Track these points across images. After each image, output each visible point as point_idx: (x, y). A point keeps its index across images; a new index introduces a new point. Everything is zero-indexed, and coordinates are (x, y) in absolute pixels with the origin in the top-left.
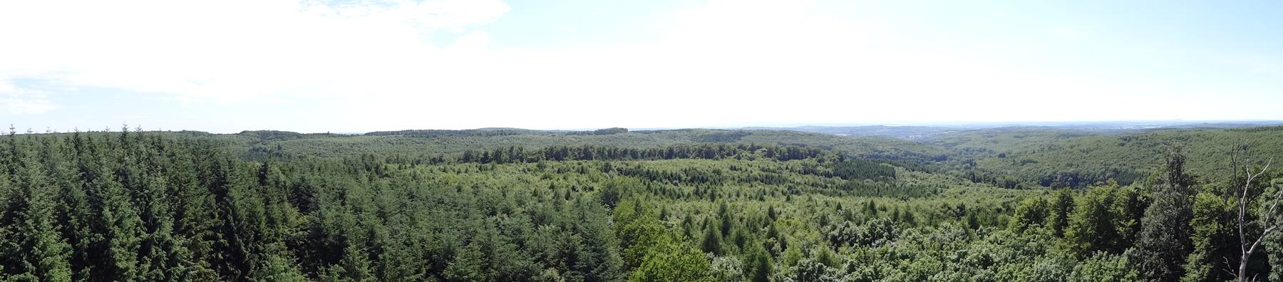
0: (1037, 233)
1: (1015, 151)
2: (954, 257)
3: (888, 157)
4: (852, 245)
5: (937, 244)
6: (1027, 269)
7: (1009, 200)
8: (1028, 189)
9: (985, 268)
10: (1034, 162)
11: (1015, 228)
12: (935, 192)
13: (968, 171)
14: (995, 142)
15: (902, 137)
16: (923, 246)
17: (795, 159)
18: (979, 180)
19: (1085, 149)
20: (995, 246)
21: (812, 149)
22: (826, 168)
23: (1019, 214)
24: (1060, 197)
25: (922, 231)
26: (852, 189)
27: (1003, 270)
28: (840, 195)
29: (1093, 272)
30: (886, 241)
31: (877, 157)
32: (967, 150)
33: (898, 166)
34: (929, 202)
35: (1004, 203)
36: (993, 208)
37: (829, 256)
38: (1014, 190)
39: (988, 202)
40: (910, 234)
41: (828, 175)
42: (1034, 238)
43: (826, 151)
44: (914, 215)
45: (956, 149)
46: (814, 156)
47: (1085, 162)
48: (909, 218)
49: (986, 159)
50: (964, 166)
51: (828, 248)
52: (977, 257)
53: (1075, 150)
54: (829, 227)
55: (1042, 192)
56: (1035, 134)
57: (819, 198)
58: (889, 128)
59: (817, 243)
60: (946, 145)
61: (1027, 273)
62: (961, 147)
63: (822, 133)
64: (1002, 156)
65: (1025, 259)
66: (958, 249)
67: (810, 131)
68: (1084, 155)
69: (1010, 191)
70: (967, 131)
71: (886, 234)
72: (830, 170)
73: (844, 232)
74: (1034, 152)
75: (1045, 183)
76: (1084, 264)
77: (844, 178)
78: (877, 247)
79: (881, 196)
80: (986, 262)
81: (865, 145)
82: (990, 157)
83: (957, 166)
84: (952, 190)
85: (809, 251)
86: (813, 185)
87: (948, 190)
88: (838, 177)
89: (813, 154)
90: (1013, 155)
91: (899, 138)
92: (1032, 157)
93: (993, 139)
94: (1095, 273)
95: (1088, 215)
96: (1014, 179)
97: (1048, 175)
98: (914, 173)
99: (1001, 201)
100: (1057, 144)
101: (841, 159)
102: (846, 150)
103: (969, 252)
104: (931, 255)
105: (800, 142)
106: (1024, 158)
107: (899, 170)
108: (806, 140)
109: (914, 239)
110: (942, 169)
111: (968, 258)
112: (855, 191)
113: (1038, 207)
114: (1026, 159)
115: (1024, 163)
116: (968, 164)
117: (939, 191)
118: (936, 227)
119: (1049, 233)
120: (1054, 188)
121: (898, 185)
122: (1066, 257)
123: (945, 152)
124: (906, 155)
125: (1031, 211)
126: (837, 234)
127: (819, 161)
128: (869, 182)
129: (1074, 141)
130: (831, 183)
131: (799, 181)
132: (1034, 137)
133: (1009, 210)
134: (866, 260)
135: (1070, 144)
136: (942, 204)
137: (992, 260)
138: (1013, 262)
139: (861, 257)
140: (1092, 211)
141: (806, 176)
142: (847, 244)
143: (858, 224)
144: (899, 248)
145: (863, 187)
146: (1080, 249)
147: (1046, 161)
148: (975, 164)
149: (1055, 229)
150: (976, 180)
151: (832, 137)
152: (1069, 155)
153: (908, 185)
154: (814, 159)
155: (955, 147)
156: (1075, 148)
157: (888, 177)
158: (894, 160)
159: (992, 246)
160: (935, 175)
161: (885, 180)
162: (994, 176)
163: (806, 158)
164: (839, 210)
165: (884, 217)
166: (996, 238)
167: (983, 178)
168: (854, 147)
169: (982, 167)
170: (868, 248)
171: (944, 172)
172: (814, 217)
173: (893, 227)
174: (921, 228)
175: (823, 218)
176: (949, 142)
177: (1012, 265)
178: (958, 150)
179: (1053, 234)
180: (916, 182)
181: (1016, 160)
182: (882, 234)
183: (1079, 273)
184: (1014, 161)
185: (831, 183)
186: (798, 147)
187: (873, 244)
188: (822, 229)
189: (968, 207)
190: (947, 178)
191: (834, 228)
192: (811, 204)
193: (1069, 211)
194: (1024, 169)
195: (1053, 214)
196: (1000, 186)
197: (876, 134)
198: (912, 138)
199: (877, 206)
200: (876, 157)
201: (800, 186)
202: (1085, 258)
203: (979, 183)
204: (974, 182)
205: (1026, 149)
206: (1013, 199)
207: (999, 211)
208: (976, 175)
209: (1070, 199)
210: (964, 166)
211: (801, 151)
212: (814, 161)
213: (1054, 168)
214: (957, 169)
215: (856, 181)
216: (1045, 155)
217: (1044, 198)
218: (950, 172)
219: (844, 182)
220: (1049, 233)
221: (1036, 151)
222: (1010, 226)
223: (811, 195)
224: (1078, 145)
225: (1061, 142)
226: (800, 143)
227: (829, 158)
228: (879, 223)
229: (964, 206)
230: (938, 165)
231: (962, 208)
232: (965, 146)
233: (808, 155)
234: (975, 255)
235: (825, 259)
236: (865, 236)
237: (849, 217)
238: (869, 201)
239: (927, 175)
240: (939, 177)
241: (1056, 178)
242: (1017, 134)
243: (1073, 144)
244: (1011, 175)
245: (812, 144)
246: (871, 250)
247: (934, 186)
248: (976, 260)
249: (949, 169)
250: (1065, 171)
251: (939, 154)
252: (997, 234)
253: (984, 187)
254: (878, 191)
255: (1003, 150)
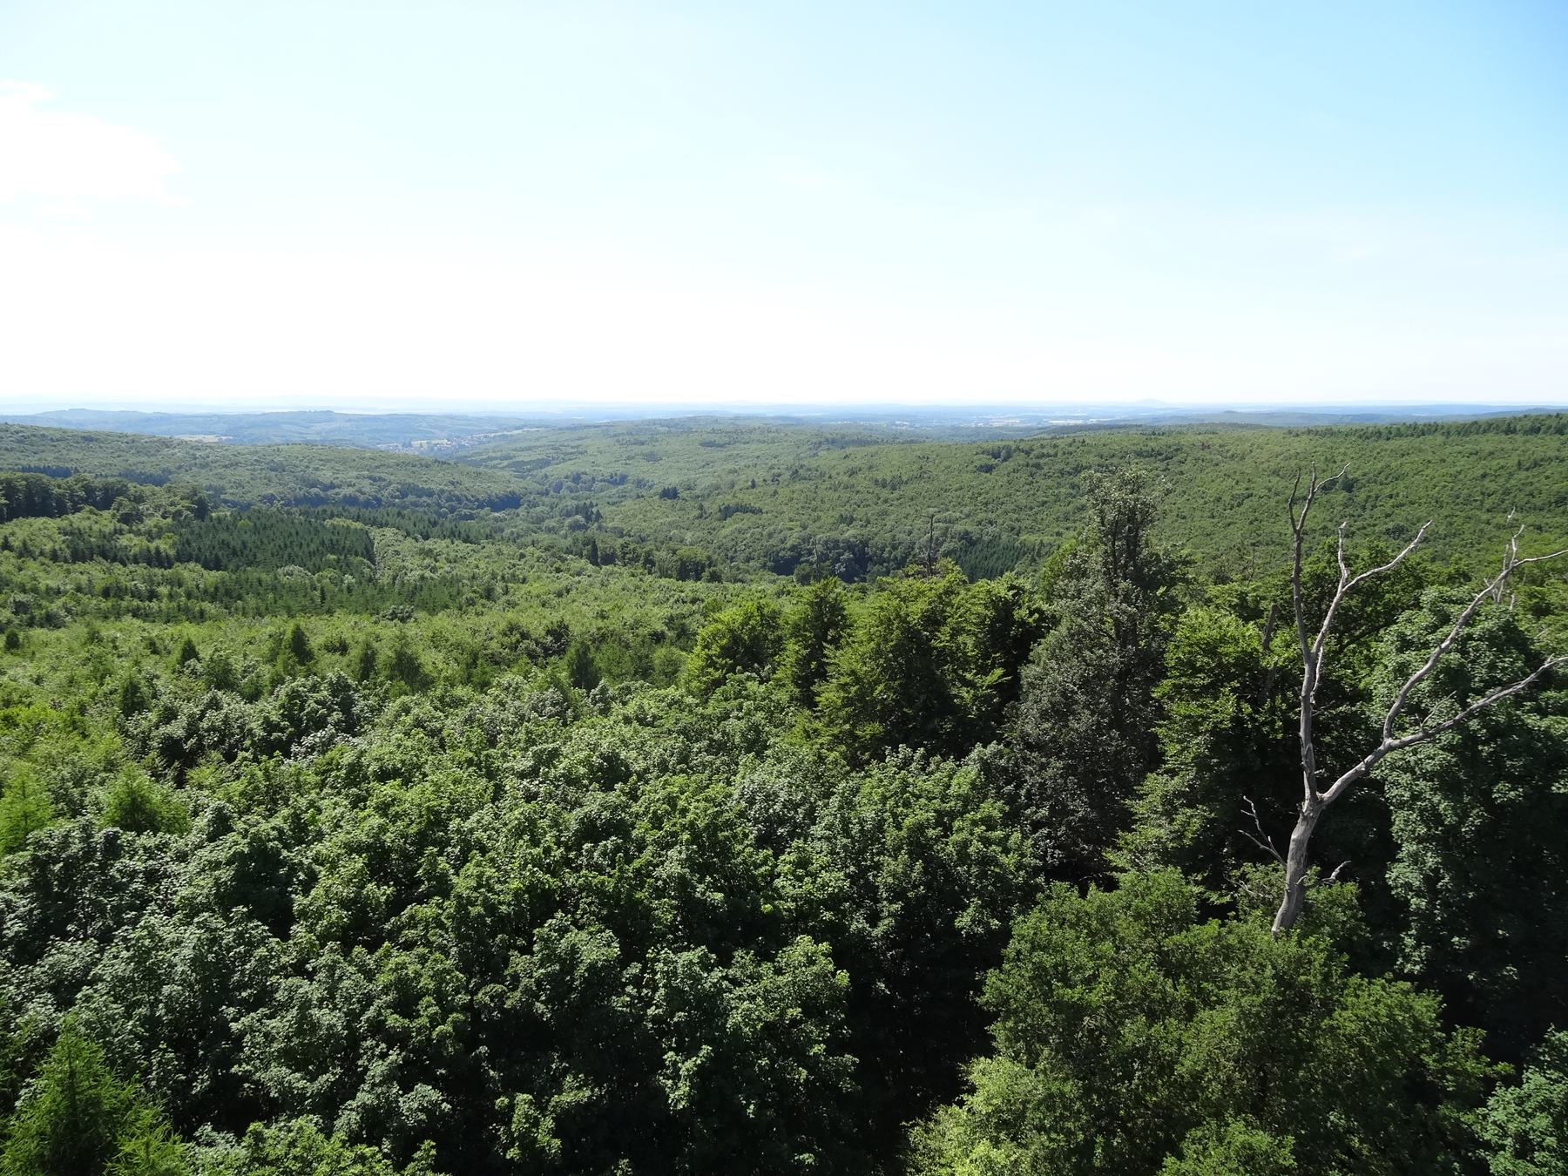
0: (747, 698)
1: (705, 481)
2: (526, 763)
3: (351, 501)
4: (230, 757)
5: (476, 734)
6: (716, 790)
7: (685, 609)
8: (736, 581)
9: (608, 788)
10: (753, 512)
11: (695, 684)
12: (489, 594)
13: (580, 534)
14: (652, 458)
15: (394, 446)
16: (442, 739)
17: (37, 515)
18: (609, 559)
19: (889, 479)
20: (636, 731)
21: (98, 483)
22: (151, 537)
23: (707, 647)
24: (811, 604)
25: (441, 699)
26: (240, 598)
27: (654, 793)
28: (201, 617)
29: (884, 799)
30: (332, 737)
31: (317, 501)
32: (577, 478)
33: (381, 526)
34: (471, 620)
35: (671, 619)
36: (640, 631)
37: (149, 801)
38: (700, 585)
39: (628, 615)
40: (407, 711)
41: (157, 560)
42: (740, 708)
43: (148, 489)
44: (422, 660)
45: (546, 476)
46: (105, 504)
47: (885, 513)
48: (408, 671)
49: (628, 503)
50: (569, 521)
51: (144, 778)
52: (586, 762)
53: (861, 481)
54: (153, 716)
55: (771, 589)
56: (755, 436)
57: (128, 632)
58: (349, 419)
59: (111, 766)
60: (518, 466)
61: (713, 800)
62: (558, 471)
63: (129, 431)
64: (670, 494)
65: (711, 763)
66: (534, 743)
67: (90, 428)
68: (885, 493)
69: (689, 585)
70: (573, 428)
71: (336, 716)
72: (164, 545)
73: (205, 724)
74: (753, 486)
75: (783, 566)
76: (864, 778)
77: (215, 565)
78: (307, 753)
79: (330, 612)
80: (611, 772)
81: (278, 468)
82: (638, 497)
83: (552, 523)
84: (535, 588)
85: (84, 794)
86: (106, 593)
87: (525, 587)
88: (192, 565)
89: (102, 498)
90: (697, 492)
91: (383, 447)
92: (749, 499)
93: (646, 449)
94: (891, 802)
95: (878, 653)
96: (701, 554)
97: (789, 544)
98: (429, 544)
99: (666, 611)
100: (813, 463)
101: (201, 510)
102: (216, 483)
103: (564, 750)
104: (460, 766)
105: (50, 459)
106: (729, 500)
107: (383, 538)
108: (74, 456)
109: (419, 723)
110: (507, 532)
111: (562, 766)
112: (252, 601)
113: (753, 628)
114: (733, 502)
115: (727, 513)
116: (578, 517)
117: (499, 590)
118: (483, 686)
119: (782, 696)
120: (804, 580)
121: (384, 579)
122: (821, 759)
123: (516, 486)
124: (404, 495)
125: (736, 639)
126: (180, 733)
127: (126, 519)
128: (292, 574)
129: (859, 456)
130: (169, 582)
131: (53, 584)
132: (754, 446)
133: (684, 636)
134: (273, 797)
135: (850, 464)
136: (503, 625)
137: (627, 767)
138: (682, 771)
139: (256, 788)
140: (886, 641)
141: (79, 566)
142: (216, 755)
143: (253, 697)
144: (375, 751)
145: (274, 589)
146: (856, 738)
147: (785, 508)
148: (599, 516)
149: (798, 686)
150: (600, 558)
151: (166, 444)
152: (845, 495)
153: (413, 576)
154: (106, 514)
155: (544, 471)
156: (860, 475)
157: (352, 558)
158: (369, 509)
159: (627, 731)
160: (490, 548)
161: (347, 568)
162: (649, 546)
163: (79, 510)
164: (192, 662)
165: (333, 668)
166: (641, 707)
167: (619, 553)
168: (243, 474)
169: (616, 523)
170: (279, 763)
171: (514, 539)
172: (106, 688)
173: (356, 696)
174: (439, 692)
175: (132, 689)
176: (524, 457)
177: (680, 779)
178: (551, 479)
179: (792, 699)
180: (434, 570)
181: (706, 504)
182: (324, 718)
183: (848, 804)
184: (701, 507)
185: (169, 582)
186: (45, 478)
187: (294, 748)
188: (130, 726)
189: (576, 629)
190: (522, 556)
191: (169, 715)
192: (97, 650)
193: (835, 642)
194: (729, 528)
195: (793, 649)
196: (664, 574)
197: (309, 438)
198: (419, 446)
199: (315, 642)
200: (315, 502)
201: (59, 602)
202: (868, 762)
203: (610, 567)
204: (595, 563)
205: (731, 477)
206: (695, 607)
207: (658, 638)
208: (600, 545)
209: (836, 609)
210: (569, 521)
211: (56, 491)
212: (106, 521)
213: (804, 527)
214: (550, 530)
215: (253, 573)
216: (784, 492)
217: (774, 604)
218: (529, 539)
219: (213, 576)
220: (782, 696)
221: (759, 481)
222: (683, 676)
223: (98, 624)
224: (871, 467)
225: (827, 459)
226: (53, 464)
227: (157, 508)
228: (314, 688)
229: (566, 627)
230: (496, 520)
231: (559, 633)
232: (568, 468)
233: (85, 501)
234: (582, 755)
235: (136, 815)
236: (270, 726)
237: (222, 679)
238: (289, 628)
239: (462, 547)
240: (499, 553)
241: (810, 553)
242: (712, 438)
243: (857, 463)
244: (692, 545)
245: (95, 468)
246: (289, 766)
247: (486, 578)
248: (582, 770)
249: (528, 532)
250: (834, 535)
251: (497, 489)
252: (647, 700)
253: (621, 577)
254: (323, 598)
255: (673, 480)
